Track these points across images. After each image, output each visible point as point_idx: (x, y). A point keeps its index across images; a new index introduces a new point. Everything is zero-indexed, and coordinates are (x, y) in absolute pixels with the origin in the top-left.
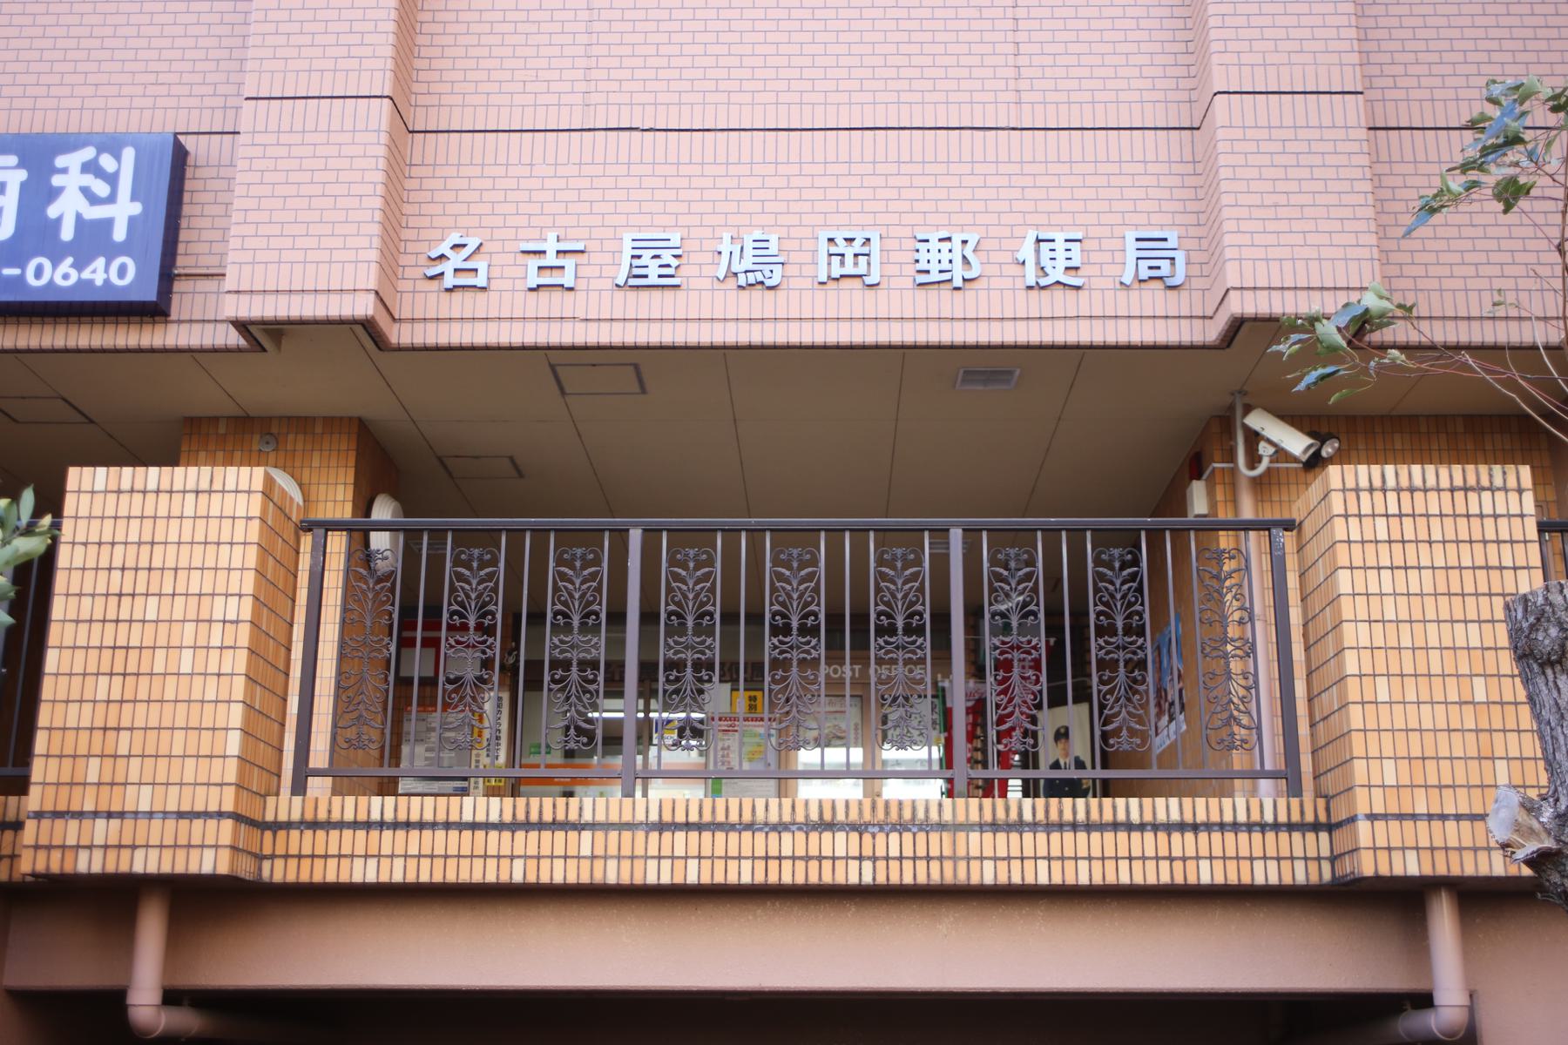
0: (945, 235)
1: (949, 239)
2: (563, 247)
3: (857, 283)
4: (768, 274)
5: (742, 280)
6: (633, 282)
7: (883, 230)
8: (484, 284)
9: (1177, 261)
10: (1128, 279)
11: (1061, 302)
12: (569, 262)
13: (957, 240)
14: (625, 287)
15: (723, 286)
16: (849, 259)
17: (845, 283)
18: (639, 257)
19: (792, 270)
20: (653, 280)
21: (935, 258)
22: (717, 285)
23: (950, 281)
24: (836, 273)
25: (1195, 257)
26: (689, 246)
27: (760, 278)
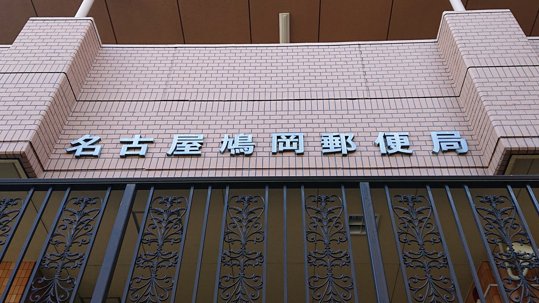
0: (337, 134)
1: (338, 136)
2: (142, 140)
3: (292, 154)
4: (246, 149)
5: (233, 152)
6: (175, 153)
7: (305, 135)
8: (144, 154)
9: (461, 143)
10: (437, 150)
11: (400, 161)
12: (144, 147)
13: (343, 136)
14: (172, 155)
15: (223, 155)
16: (288, 144)
17: (285, 154)
18: (181, 143)
19: (257, 149)
20: (187, 152)
21: (332, 144)
22: (220, 155)
23: (341, 152)
24: (281, 148)
25: (471, 142)
26: (207, 140)
27: (242, 151)
